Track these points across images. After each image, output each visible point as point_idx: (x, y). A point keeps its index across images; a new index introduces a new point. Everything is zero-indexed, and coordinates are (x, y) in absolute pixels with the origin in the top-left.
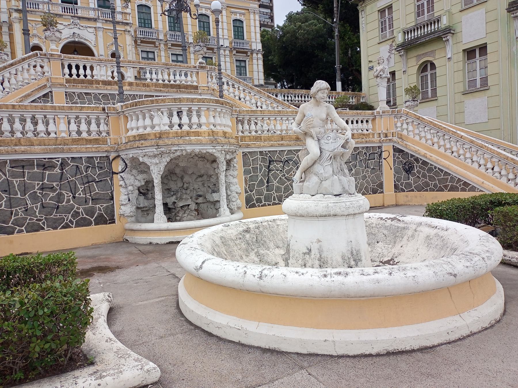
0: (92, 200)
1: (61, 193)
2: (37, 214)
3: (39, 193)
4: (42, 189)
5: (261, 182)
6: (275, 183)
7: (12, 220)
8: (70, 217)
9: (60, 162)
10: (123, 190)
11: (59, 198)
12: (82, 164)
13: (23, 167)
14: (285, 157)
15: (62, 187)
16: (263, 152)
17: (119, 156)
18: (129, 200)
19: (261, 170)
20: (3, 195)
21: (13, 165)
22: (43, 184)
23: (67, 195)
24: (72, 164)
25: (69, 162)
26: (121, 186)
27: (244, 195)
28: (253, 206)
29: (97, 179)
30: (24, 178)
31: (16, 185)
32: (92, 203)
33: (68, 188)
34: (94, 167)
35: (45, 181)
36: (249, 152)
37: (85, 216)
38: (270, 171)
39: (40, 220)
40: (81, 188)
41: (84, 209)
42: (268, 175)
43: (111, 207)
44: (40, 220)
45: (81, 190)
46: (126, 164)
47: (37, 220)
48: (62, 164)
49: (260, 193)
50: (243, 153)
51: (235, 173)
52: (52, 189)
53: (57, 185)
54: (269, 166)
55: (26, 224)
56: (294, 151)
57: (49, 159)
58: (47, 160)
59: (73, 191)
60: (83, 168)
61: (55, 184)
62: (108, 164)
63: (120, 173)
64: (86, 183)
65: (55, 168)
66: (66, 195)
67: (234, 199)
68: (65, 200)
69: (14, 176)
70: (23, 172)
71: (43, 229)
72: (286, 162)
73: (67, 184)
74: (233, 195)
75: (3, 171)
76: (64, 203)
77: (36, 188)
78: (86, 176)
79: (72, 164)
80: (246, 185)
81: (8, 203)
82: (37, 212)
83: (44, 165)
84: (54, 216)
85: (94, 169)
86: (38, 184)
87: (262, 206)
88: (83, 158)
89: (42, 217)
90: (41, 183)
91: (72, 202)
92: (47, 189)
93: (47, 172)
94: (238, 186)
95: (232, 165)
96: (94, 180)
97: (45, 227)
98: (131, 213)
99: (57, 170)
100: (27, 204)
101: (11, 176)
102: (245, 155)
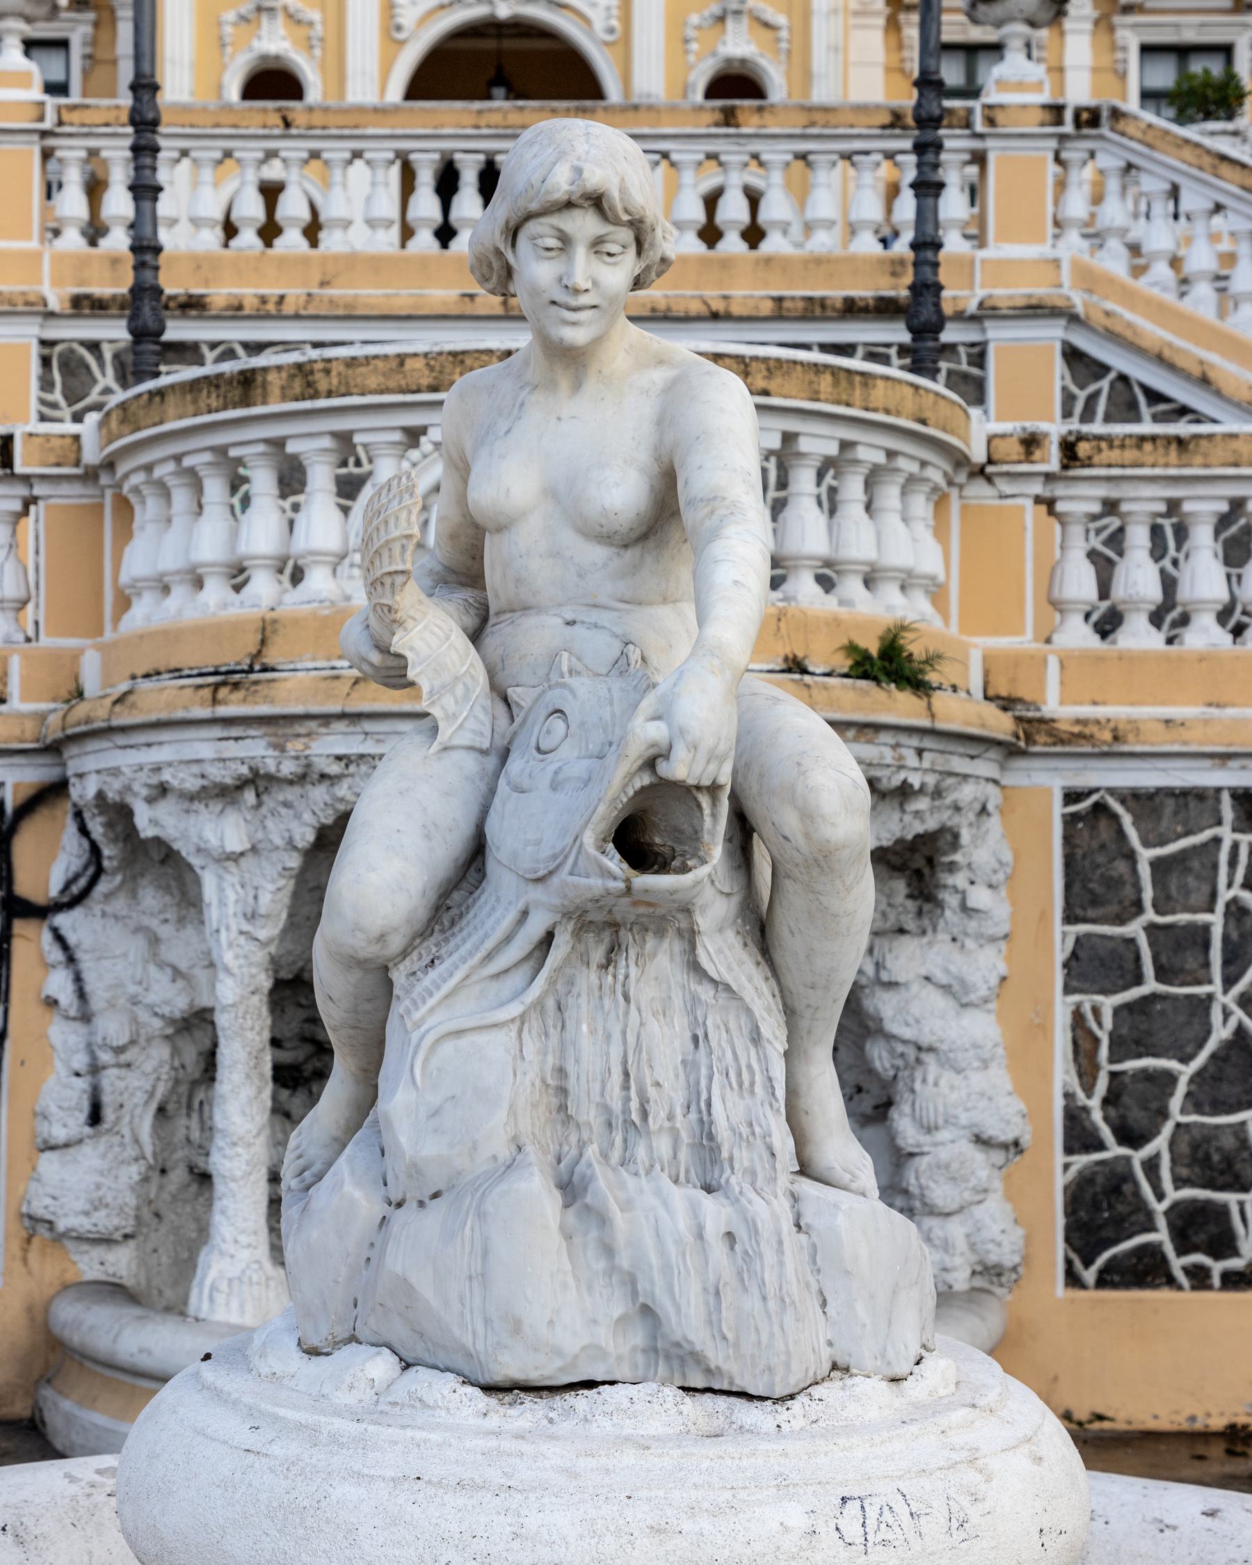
17: (55, 790)
27: (1058, 1170)
28: (1145, 1271)
36: (1137, 799)
46: (95, 850)
51: (983, 967)
74: (944, 1154)
87: (1233, 1281)
94: (999, 1078)
95: (951, 900)
102: (1089, 819)
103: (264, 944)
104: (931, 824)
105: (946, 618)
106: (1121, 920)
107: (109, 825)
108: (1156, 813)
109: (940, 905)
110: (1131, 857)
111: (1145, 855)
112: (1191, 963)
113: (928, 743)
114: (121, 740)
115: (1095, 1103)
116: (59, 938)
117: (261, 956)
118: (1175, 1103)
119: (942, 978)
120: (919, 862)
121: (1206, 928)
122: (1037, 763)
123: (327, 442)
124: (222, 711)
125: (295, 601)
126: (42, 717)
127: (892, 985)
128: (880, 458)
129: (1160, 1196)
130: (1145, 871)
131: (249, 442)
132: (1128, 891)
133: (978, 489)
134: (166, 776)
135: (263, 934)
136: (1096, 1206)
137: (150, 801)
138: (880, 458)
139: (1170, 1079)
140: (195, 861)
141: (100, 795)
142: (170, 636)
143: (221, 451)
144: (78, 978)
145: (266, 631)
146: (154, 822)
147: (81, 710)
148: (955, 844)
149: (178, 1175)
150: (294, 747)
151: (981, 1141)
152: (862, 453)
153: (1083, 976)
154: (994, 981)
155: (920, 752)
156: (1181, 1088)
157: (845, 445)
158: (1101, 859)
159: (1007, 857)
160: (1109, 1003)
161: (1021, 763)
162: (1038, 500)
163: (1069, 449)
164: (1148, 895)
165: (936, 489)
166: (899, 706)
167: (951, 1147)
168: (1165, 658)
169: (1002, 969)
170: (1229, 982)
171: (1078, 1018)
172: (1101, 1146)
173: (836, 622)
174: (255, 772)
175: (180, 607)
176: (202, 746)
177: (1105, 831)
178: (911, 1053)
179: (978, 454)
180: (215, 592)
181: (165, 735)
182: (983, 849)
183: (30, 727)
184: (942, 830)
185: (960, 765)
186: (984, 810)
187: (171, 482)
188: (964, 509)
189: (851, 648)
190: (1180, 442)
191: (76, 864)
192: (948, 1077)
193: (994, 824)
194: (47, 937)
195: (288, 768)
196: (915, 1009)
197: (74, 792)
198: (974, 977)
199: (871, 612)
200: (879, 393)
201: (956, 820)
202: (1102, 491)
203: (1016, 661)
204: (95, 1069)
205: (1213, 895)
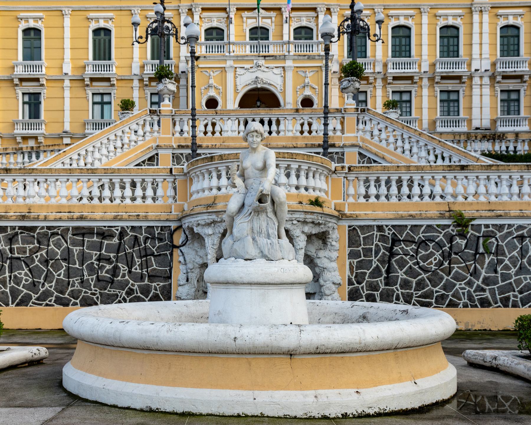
0: (149, 276)
1: (117, 266)
2: (92, 287)
3: (96, 264)
4: (99, 259)
5: (377, 272)
6: (401, 274)
7: (68, 291)
8: (124, 295)
9: (119, 231)
10: (182, 267)
11: (115, 271)
12: (142, 234)
13: (83, 235)
14: (421, 235)
15: (119, 259)
16: (382, 226)
17: (180, 227)
18: (187, 280)
19: (377, 253)
20: (64, 264)
21: (75, 232)
22: (100, 254)
23: (123, 268)
24: (131, 234)
25: (128, 231)
26: (180, 262)
27: (347, 288)
29: (155, 252)
30: (83, 247)
31: (76, 254)
32: (148, 280)
33: (125, 261)
34: (153, 238)
35: (103, 252)
36: (361, 227)
37: (139, 294)
38: (392, 255)
39: (94, 294)
40: (138, 261)
41: (139, 286)
42: (390, 260)
43: (168, 287)
44: (94, 294)
45: (138, 264)
46: (187, 236)
47: (92, 294)
48: (121, 233)
49: (373, 287)
50: (349, 227)
51: (334, 255)
52: (108, 260)
53: (114, 257)
54: (392, 248)
55: (81, 297)
56: (438, 226)
57: (109, 227)
58: (107, 228)
59: (130, 265)
60: (141, 238)
61: (112, 255)
62: (170, 236)
63: (181, 246)
64: (144, 256)
65: (114, 237)
66: (122, 268)
67: (327, 292)
68: (121, 274)
69: (74, 244)
70: (83, 240)
71: (96, 304)
72: (423, 244)
73: (124, 257)
74: (328, 286)
75: (66, 238)
76: (119, 278)
77: (94, 258)
78: (145, 249)
79: (131, 234)
80: (352, 273)
81: (67, 273)
82: (92, 285)
83: (104, 233)
84: (109, 291)
85: (153, 241)
86: (96, 254)
88: (143, 228)
89: (96, 291)
90: (99, 253)
91: (127, 277)
92: (104, 261)
93: (106, 242)
94: (337, 273)
95: (329, 244)
96: (153, 254)
97: (99, 303)
98: (188, 296)
99: (116, 240)
100: (83, 276)
101: (72, 244)
102: (352, 230)
103: (215, 249)
104: (324, 230)
105: (328, 197)
106: (358, 247)
107: (189, 232)
108: (363, 229)
109: (327, 245)
110: (359, 237)
111: (362, 236)
112: (369, 254)
113: (323, 216)
114: (192, 217)
115: (353, 277)
116: (181, 251)
117: (214, 251)
118: (366, 277)
119: (327, 256)
120: (324, 238)
121: (372, 248)
122: (343, 221)
123: (225, 168)
124: (208, 211)
125: (220, 193)
126: (178, 215)
127: (319, 258)
128: (315, 169)
129: (364, 293)
130: (362, 239)
131: (212, 168)
132: (359, 242)
133: (334, 176)
134: (199, 222)
135: (215, 248)
136: (353, 294)
137: (196, 227)
138: (315, 169)
139: (366, 273)
140: (204, 236)
141: (188, 226)
142: (200, 200)
143: (208, 169)
144: (184, 258)
145: (215, 198)
146: (197, 230)
147: (185, 212)
148: (329, 234)
149: (201, 292)
150: (220, 216)
151: (334, 283)
152: (312, 169)
153: (351, 256)
154: (336, 257)
155: (321, 217)
156: (368, 275)
157: (309, 167)
158: (354, 237)
159: (338, 236)
160: (355, 261)
161: (341, 221)
162: (344, 177)
163: (349, 168)
164: (362, 243)
165: (326, 175)
166: (318, 209)
167: (329, 284)
168: (366, 203)
169: (338, 255)
170: (375, 257)
171: (350, 263)
172: (354, 285)
173: (307, 196)
174: (214, 221)
175: (201, 195)
176: (205, 217)
177: (355, 232)
178: (322, 269)
179: (333, 169)
180: (207, 193)
181: (199, 215)
182: (334, 235)
183: (176, 217)
184: (326, 231)
185: (329, 220)
186: (334, 228)
187: (199, 175)
188: (332, 179)
189: (310, 200)
190: (368, 167)
191: (184, 239)
192: (328, 273)
193: (336, 231)
194: (179, 251)
195: (219, 220)
196: (323, 262)
197: (183, 227)
198: (333, 256)
199: (313, 194)
200: (315, 159)
201: (329, 229)
202: (355, 176)
203: (340, 204)
204: (187, 273)
205: (373, 243)
